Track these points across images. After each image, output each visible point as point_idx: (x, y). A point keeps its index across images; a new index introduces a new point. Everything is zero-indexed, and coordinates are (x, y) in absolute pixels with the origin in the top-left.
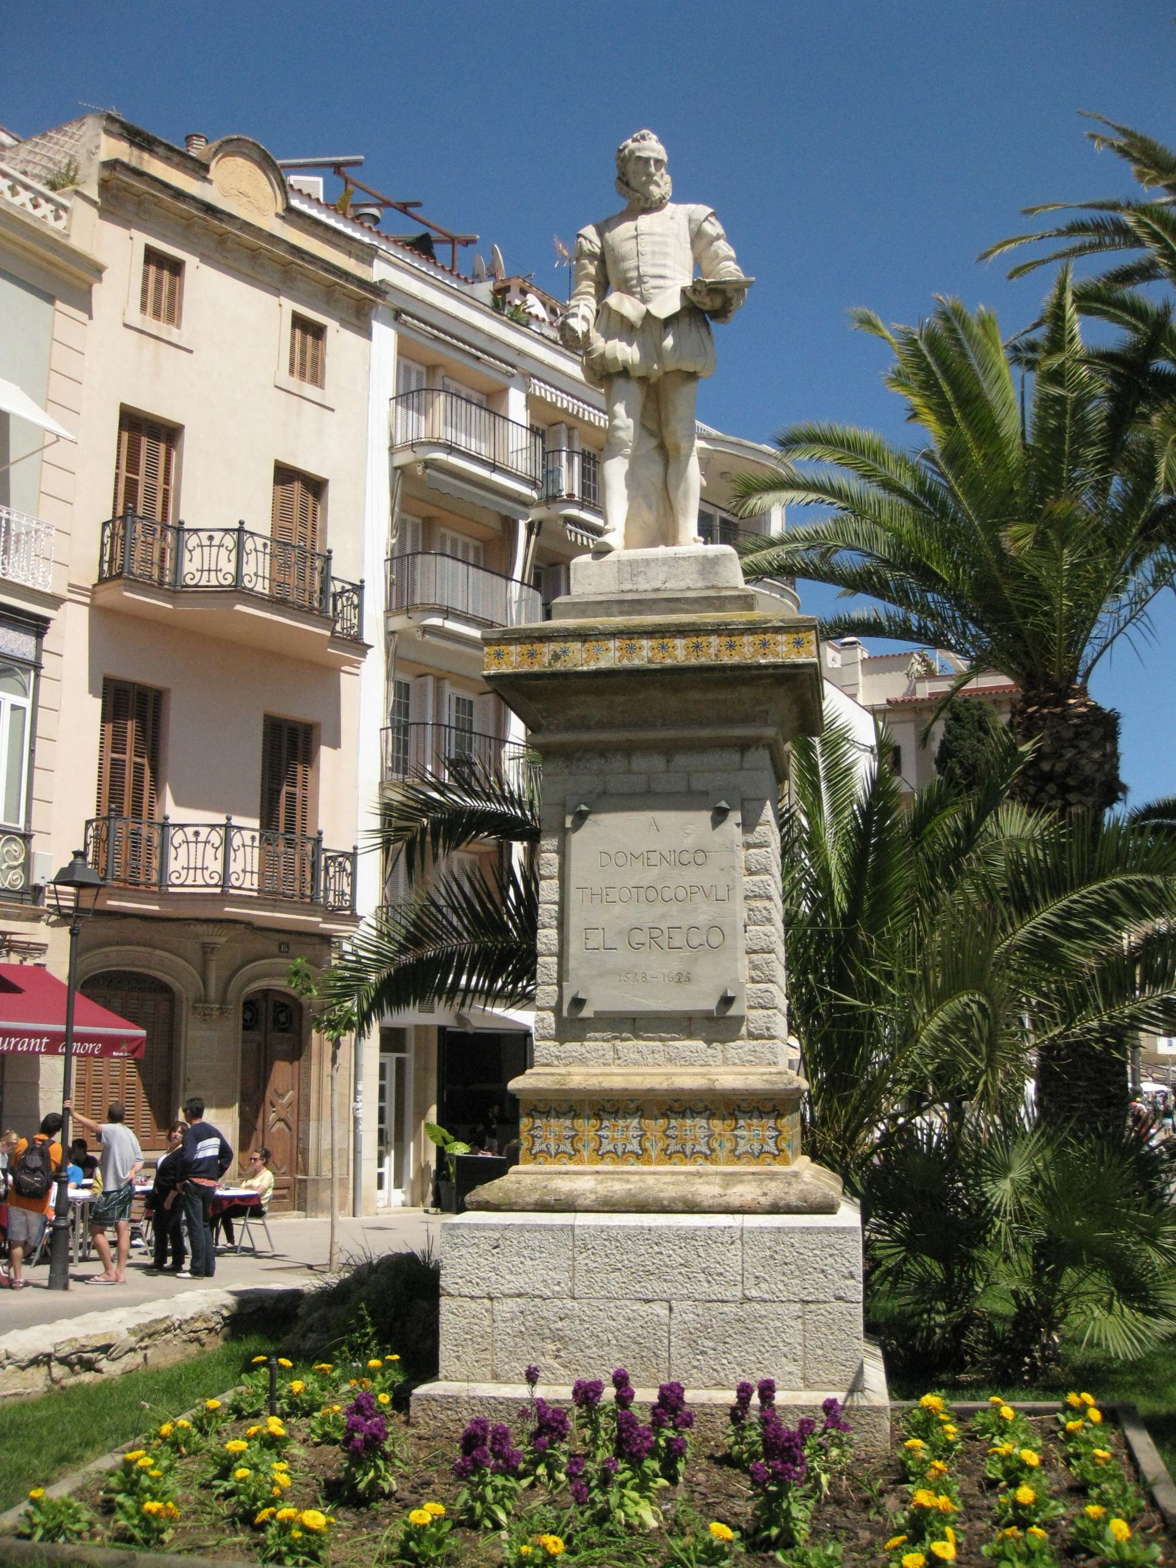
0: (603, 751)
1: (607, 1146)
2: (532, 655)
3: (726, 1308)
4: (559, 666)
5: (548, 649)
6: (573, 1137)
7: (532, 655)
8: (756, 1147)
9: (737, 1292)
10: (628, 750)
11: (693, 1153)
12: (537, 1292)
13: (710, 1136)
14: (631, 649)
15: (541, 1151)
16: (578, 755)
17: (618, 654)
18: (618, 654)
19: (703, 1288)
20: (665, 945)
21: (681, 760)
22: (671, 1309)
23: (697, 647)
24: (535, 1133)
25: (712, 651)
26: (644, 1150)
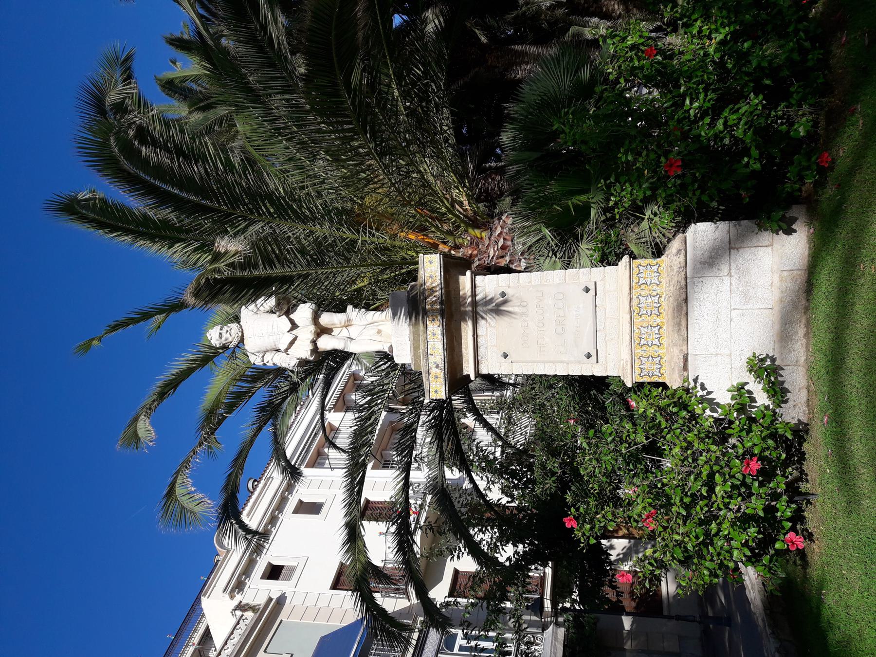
1: (656, 342)
2: (436, 377)
4: (441, 365)
5: (434, 371)
12: (729, 371)
14: (434, 334)
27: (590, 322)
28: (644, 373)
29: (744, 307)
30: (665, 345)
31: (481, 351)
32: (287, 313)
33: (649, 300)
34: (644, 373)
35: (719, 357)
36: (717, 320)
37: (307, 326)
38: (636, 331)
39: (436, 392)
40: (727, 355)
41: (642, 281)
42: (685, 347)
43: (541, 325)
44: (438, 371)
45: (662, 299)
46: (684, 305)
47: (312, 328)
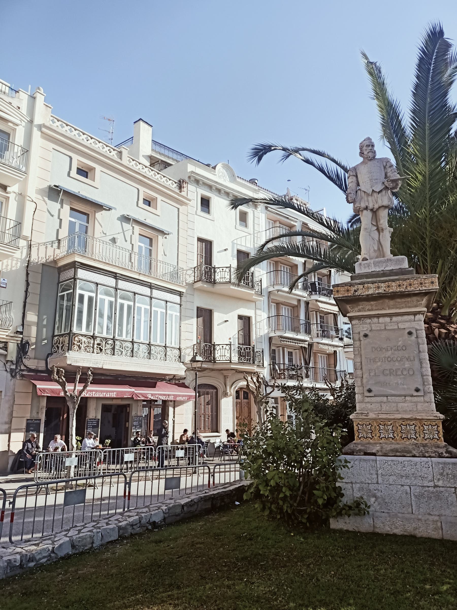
0: (370, 317)
2: (348, 291)
3: (430, 488)
5: (353, 289)
6: (371, 432)
8: (431, 437)
9: (431, 484)
10: (378, 316)
11: (410, 438)
12: (367, 482)
13: (416, 433)
14: (378, 287)
15: (362, 437)
16: (362, 319)
17: (374, 289)
18: (374, 289)
20: (395, 374)
21: (394, 319)
22: (410, 488)
24: (359, 431)
25: (404, 287)
26: (395, 437)
27: (393, 392)
28: (360, 427)
29: (412, 495)
30: (381, 441)
33: (412, 432)
34: (360, 427)
35: (376, 476)
36: (402, 477)
38: (389, 423)
40: (378, 481)
42: (380, 453)
43: (389, 359)
45: (413, 440)
46: (411, 455)
47: (376, 206)
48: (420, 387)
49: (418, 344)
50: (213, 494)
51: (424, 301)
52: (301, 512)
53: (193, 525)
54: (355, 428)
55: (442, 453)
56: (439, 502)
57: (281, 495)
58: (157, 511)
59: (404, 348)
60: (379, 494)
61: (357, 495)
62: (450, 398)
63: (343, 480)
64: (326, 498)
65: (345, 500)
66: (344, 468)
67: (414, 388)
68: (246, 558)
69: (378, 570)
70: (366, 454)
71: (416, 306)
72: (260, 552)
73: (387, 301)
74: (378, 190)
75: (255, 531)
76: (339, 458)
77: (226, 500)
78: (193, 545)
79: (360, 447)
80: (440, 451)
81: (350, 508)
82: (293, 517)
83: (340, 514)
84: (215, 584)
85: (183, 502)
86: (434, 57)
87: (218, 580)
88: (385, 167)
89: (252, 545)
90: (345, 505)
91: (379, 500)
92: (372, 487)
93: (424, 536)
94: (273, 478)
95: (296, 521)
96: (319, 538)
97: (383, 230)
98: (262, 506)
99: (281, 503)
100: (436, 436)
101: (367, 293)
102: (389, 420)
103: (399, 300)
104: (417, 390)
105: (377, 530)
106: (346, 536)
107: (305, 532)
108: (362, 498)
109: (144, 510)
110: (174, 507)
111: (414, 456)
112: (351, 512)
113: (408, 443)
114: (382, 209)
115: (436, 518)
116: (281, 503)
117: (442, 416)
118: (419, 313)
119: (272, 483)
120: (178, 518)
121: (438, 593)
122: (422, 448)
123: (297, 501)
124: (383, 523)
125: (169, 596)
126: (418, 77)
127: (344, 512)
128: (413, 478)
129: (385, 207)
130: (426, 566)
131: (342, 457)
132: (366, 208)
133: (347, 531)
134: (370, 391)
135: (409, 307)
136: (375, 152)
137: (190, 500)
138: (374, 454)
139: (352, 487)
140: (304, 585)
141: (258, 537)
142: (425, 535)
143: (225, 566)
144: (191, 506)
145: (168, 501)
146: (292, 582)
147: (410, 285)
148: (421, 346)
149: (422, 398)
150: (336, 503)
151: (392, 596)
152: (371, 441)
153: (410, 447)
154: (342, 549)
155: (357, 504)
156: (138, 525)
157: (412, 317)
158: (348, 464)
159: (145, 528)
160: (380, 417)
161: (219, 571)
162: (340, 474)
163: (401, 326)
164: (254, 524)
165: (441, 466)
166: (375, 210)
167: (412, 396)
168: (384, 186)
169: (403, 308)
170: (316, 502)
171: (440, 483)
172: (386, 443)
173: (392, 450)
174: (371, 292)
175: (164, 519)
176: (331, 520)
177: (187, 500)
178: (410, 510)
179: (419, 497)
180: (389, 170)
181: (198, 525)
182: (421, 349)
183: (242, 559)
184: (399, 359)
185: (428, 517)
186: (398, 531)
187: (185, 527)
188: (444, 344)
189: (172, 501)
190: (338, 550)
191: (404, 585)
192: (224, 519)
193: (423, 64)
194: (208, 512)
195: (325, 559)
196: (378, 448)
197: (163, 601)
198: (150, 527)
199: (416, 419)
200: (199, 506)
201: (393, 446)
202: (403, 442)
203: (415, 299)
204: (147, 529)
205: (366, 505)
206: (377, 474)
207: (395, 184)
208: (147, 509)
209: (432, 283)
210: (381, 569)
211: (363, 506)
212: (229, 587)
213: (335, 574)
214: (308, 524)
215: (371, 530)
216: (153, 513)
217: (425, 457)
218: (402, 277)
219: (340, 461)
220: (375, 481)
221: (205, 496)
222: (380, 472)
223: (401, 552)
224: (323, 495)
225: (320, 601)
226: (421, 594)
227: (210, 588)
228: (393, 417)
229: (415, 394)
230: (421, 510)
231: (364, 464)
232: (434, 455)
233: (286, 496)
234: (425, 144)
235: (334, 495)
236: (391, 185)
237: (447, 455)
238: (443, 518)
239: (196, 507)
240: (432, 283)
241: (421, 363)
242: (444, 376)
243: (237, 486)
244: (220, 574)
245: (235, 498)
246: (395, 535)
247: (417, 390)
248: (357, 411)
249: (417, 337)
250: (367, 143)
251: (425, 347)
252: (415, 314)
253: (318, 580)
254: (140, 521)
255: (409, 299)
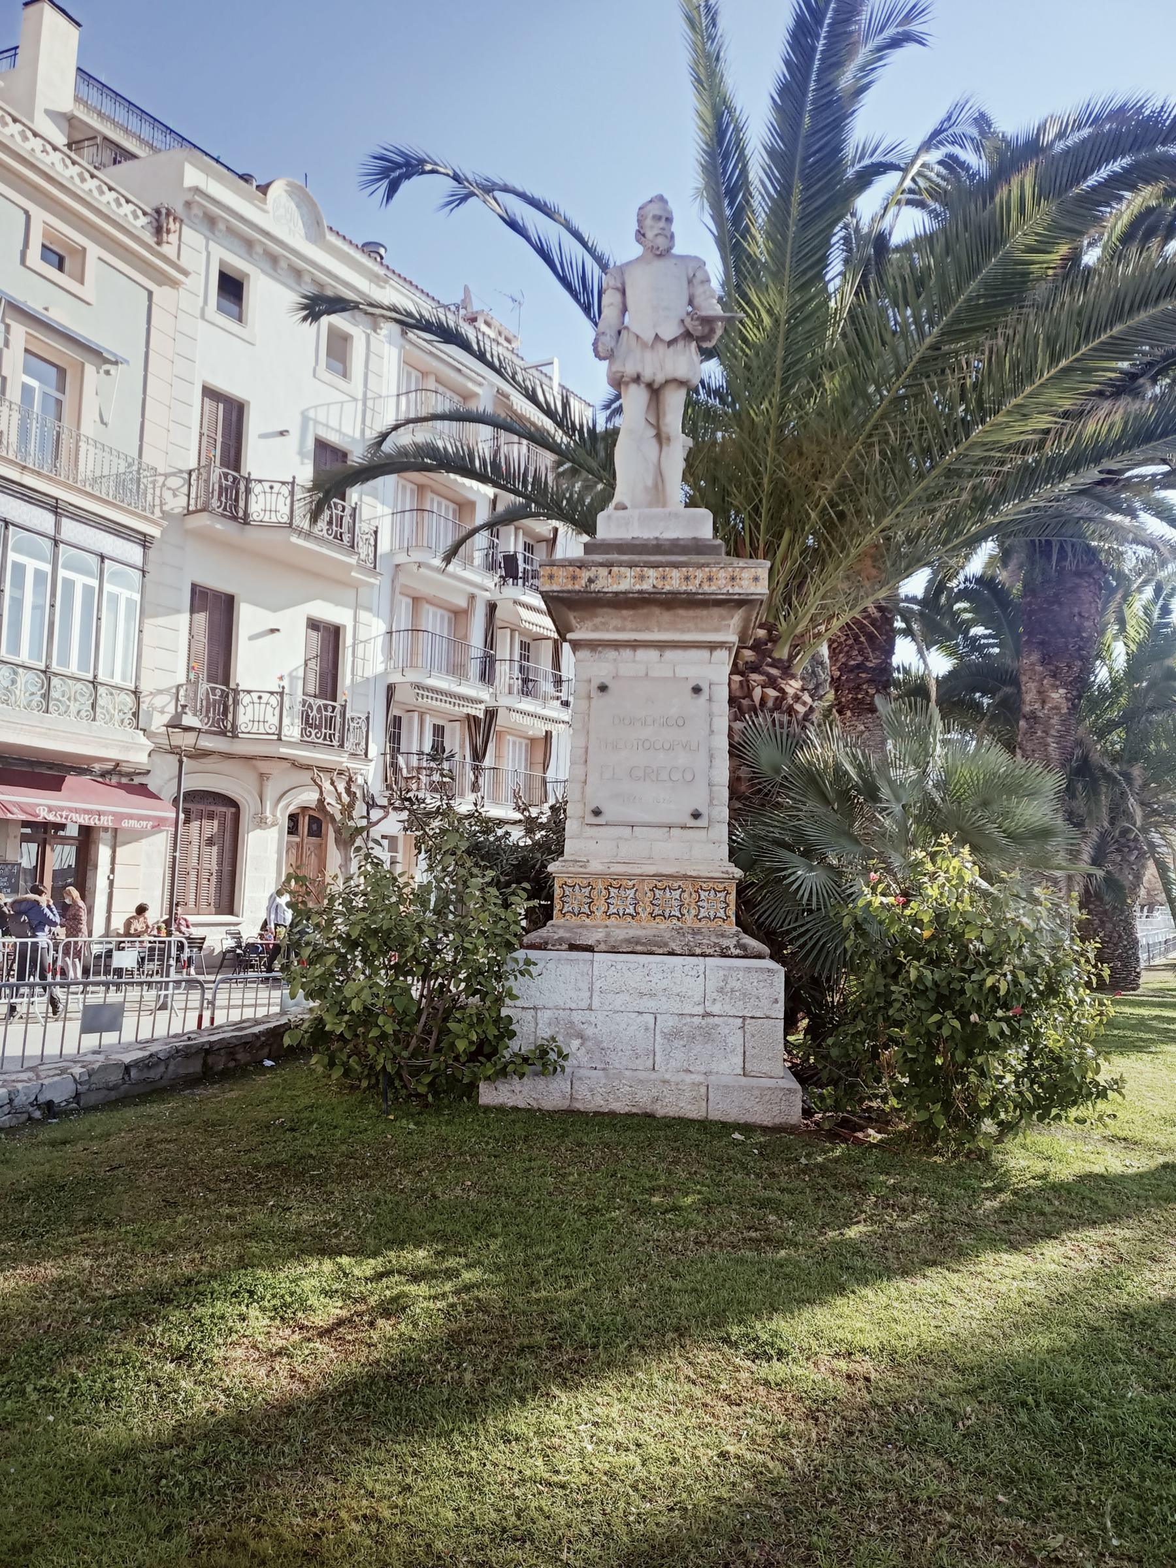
0: (616, 645)
1: (613, 910)
2: (574, 578)
5: (585, 575)
7: (574, 578)
9: (699, 1010)
10: (634, 645)
14: (642, 578)
19: (676, 1007)
21: (670, 654)
23: (687, 578)
25: (697, 582)
27: (647, 818)
30: (608, 922)
31: (612, 654)
32: (688, 335)
33: (676, 903)
37: (662, 368)
39: (551, 577)
41: (703, 894)
42: (603, 947)
43: (647, 745)
44: (583, 582)
46: (666, 950)
47: (660, 379)
48: (703, 810)
49: (711, 715)
50: (209, 1042)
51: (736, 620)
52: (416, 1072)
53: (153, 1109)
54: (558, 892)
55: (728, 948)
56: (709, 1046)
57: (374, 1033)
58: (56, 1078)
59: (681, 722)
60: (589, 1031)
61: (545, 1032)
62: (763, 839)
63: (518, 1003)
64: (475, 1038)
65: (514, 1045)
66: (522, 974)
67: (690, 810)
68: (278, 1164)
69: (564, 1176)
70: (573, 947)
71: (717, 630)
72: (313, 1152)
73: (657, 611)
74: (668, 338)
75: (306, 1114)
76: (515, 955)
77: (239, 1057)
78: (149, 1146)
79: (562, 933)
80: (725, 942)
81: (526, 1060)
82: (397, 1083)
83: (503, 1073)
84: (199, 1213)
85: (128, 1058)
86: (827, 21)
87: (208, 1207)
88: (690, 282)
89: (294, 1139)
90: (516, 1055)
91: (589, 1044)
92: (577, 1017)
93: (671, 1114)
94: (357, 995)
95: (404, 1091)
96: (448, 1123)
97: (668, 439)
98: (326, 1060)
99: (371, 1050)
100: (721, 914)
101: (615, 588)
102: (630, 877)
103: (682, 612)
104: (696, 815)
105: (579, 1106)
106: (512, 1117)
107: (420, 1113)
108: (553, 1039)
109: (24, 1076)
110: (104, 1068)
111: (672, 953)
112: (527, 1069)
113: (662, 926)
114: (672, 386)
115: (701, 1078)
116: (371, 1050)
117: (738, 873)
118: (721, 645)
119: (355, 1006)
120: (113, 1095)
121: (675, 1208)
122: (690, 937)
123: (411, 1048)
124: (591, 1090)
125: (83, 1241)
126: (788, 63)
127: (510, 1068)
128: (664, 999)
129: (681, 383)
130: (662, 1166)
131: (520, 954)
132: (637, 379)
133: (515, 1109)
134: (597, 813)
135: (703, 631)
136: (672, 236)
137: (147, 1053)
138: (589, 949)
139: (535, 1018)
140: (401, 1208)
141: (311, 1123)
142: (672, 1112)
143: (225, 1181)
144: (148, 1067)
145: (90, 1058)
146: (378, 1202)
147: (710, 579)
148: (715, 720)
149: (704, 832)
150: (495, 1052)
151: (583, 1218)
152: (588, 921)
153: (667, 935)
154: (497, 1140)
155: (543, 1052)
156: (6, 1109)
157: (705, 654)
158: (531, 968)
159: (25, 1116)
160: (612, 870)
161: (211, 1191)
162: (510, 988)
163: (682, 672)
164: (306, 1101)
165: (722, 973)
166: (656, 386)
167: (684, 827)
168: (682, 330)
169: (689, 631)
170: (452, 1046)
171: (716, 1009)
172: (617, 927)
173: (628, 941)
174: (624, 586)
175: (77, 1096)
176: (483, 1086)
177: (140, 1054)
178: (649, 1063)
179: (673, 1035)
180: (699, 290)
181: (163, 1109)
182: (715, 727)
183: (269, 1166)
184: (667, 746)
185: (683, 1075)
186: (620, 1107)
187: (130, 1114)
188: (769, 720)
189: (101, 1058)
190: (487, 1143)
191: (611, 1197)
192: (233, 1094)
193: (802, 34)
194: (192, 1082)
195: (458, 1159)
196: (600, 935)
197: (67, 1251)
198: (37, 1114)
199: (685, 877)
200: (171, 1068)
201: (632, 933)
202: (653, 923)
203: (716, 612)
204: (30, 1119)
205: (560, 1054)
206: (591, 990)
207: (707, 330)
208: (31, 1074)
209: (756, 579)
210: (571, 1174)
211: (553, 1056)
212: (231, 1218)
213: (474, 1185)
214: (430, 1098)
215: (564, 1104)
216: (46, 1082)
217: (693, 955)
218: (695, 558)
219: (516, 961)
220: (584, 1005)
221: (187, 1046)
222: (597, 985)
223: (619, 1144)
224: (468, 1032)
225: (433, 1234)
226: (641, 1211)
227: (186, 1222)
228: (638, 871)
229: (692, 823)
230: (673, 1063)
231: (566, 969)
232: (711, 951)
233: (384, 1036)
234: (785, 238)
235: (492, 1032)
236: (698, 330)
237: (738, 952)
238: (712, 1078)
239: (162, 1069)
240: (756, 579)
241: (711, 757)
242: (760, 790)
243: (271, 1025)
244: (211, 1197)
245: (266, 1050)
246: (612, 1114)
247: (696, 815)
248: (566, 856)
249: (710, 700)
250: (655, 209)
251: (722, 723)
252: (712, 647)
253: (434, 1197)
254: (11, 1100)
255: (705, 612)
